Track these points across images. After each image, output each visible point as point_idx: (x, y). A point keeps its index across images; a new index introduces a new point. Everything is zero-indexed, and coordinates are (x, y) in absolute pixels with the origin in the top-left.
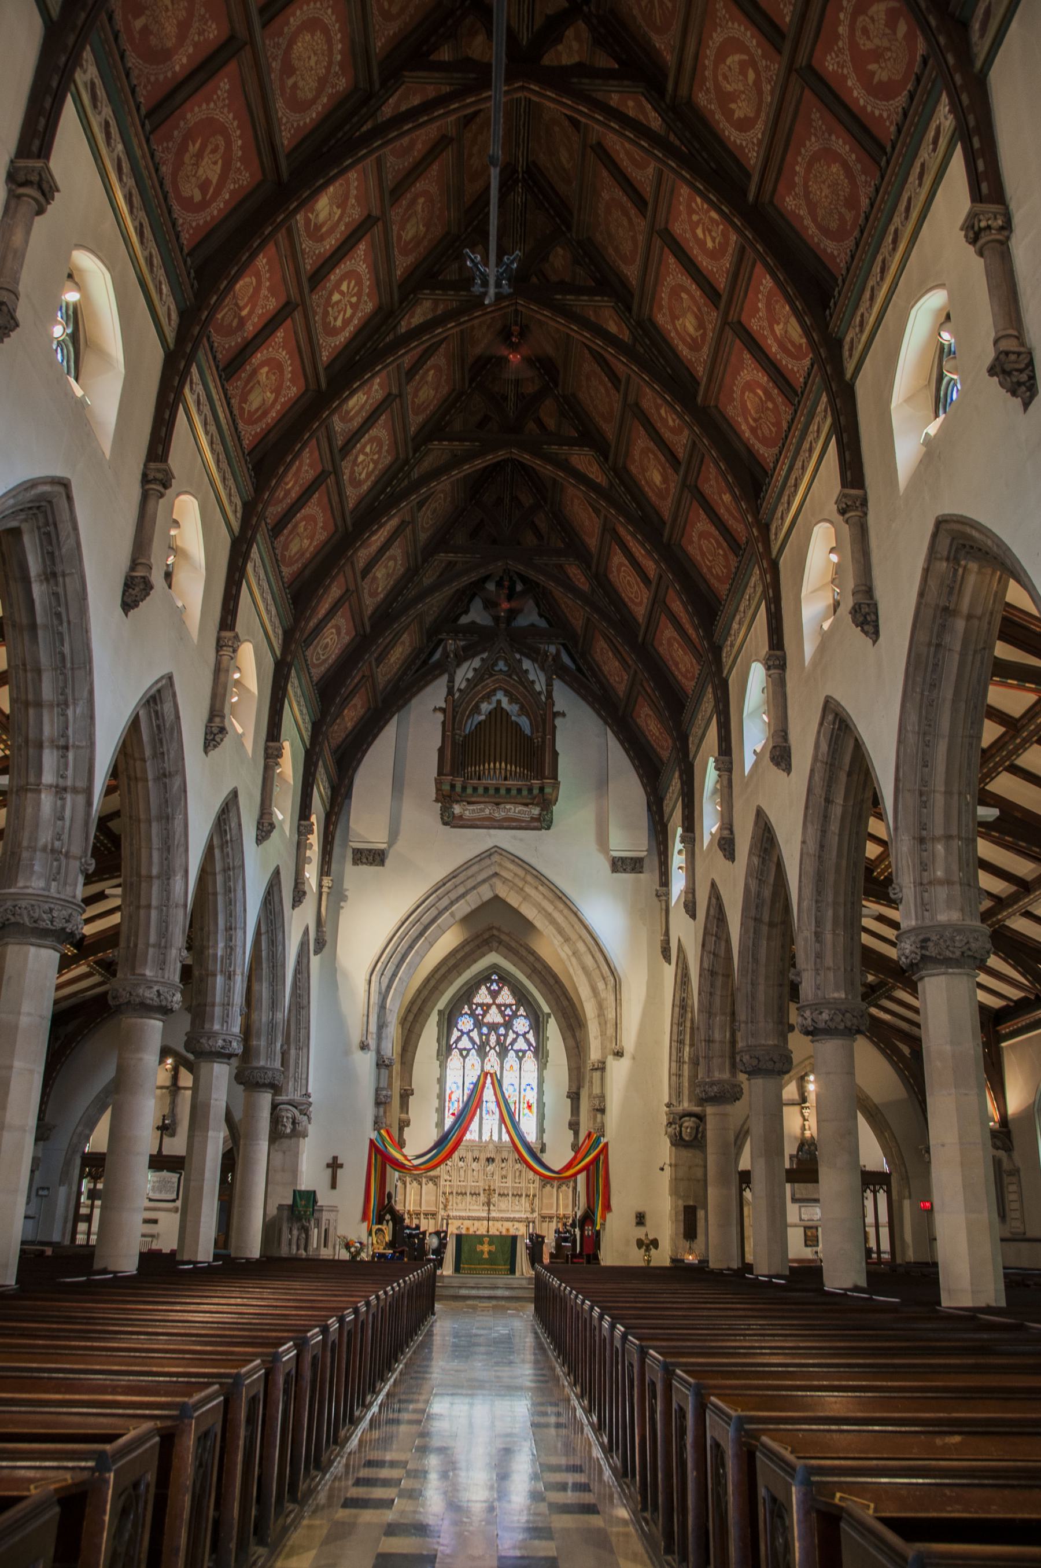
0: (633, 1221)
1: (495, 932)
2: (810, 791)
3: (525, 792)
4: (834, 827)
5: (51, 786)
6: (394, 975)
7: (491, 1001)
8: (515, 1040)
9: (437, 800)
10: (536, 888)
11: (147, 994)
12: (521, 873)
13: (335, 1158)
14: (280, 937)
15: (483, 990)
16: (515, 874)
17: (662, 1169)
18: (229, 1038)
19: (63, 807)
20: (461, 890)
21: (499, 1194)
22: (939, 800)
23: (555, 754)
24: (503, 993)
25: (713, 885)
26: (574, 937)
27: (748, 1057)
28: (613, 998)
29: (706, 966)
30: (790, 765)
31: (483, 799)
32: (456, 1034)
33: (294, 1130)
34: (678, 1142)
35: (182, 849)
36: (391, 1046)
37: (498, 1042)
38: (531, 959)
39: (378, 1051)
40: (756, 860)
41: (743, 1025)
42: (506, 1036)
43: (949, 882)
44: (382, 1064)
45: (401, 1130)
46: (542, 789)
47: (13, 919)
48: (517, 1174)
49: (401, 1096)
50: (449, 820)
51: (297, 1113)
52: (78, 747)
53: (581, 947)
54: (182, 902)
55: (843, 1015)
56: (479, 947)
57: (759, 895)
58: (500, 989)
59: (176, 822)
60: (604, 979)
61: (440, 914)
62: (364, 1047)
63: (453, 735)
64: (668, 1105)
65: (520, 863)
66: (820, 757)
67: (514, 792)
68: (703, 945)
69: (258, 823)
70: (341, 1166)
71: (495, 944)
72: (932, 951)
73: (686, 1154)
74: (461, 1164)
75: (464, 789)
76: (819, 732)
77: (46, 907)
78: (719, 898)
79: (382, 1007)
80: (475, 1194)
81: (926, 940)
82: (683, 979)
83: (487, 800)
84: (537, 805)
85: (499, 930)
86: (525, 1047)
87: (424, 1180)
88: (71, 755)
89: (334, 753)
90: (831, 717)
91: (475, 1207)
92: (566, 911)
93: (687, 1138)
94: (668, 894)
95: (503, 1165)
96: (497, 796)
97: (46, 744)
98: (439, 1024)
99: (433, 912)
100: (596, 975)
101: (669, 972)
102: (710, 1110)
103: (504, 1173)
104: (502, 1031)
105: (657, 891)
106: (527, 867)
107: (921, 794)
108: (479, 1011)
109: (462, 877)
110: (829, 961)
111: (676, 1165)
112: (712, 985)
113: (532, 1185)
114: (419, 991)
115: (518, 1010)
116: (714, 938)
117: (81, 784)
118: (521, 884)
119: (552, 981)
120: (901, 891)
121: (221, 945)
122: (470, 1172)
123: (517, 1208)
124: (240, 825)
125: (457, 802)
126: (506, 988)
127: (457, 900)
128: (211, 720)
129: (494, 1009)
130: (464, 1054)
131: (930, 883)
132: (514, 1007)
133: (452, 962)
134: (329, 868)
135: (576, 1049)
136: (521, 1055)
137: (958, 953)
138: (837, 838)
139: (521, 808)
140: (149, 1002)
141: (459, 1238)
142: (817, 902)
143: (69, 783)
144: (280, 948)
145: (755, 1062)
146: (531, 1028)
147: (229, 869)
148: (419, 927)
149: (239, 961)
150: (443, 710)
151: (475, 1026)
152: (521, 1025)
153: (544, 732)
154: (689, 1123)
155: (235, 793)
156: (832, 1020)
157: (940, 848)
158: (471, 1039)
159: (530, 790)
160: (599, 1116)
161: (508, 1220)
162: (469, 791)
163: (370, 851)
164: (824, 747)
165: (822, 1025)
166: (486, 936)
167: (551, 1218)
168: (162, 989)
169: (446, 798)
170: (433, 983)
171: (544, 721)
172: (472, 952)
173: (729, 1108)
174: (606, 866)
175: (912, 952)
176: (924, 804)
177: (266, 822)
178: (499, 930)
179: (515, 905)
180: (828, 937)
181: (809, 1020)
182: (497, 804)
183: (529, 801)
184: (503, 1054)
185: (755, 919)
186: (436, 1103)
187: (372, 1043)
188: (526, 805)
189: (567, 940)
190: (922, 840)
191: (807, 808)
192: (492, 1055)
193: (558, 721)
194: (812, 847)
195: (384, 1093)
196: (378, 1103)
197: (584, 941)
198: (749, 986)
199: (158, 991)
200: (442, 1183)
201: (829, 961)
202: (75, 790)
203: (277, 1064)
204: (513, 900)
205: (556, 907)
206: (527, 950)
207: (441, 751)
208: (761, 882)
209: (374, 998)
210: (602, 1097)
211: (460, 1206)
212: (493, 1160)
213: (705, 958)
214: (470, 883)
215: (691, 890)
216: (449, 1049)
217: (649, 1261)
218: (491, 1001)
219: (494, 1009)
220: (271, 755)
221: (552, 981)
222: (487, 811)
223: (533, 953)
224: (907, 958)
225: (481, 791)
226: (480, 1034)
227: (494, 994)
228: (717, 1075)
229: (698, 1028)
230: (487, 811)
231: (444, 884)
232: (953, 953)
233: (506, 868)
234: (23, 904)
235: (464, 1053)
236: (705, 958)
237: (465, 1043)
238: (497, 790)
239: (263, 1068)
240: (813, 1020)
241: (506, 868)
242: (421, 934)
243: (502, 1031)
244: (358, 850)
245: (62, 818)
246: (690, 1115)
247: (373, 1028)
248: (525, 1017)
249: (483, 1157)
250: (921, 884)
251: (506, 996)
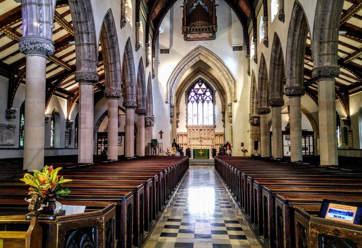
0: (241, 145)
1: (200, 69)
2: (290, 28)
3: (207, 30)
4: (297, 38)
5: (86, 44)
6: (173, 83)
7: (199, 88)
8: (206, 98)
9: (183, 34)
10: (211, 57)
11: (114, 93)
12: (207, 53)
13: (161, 131)
14: (143, 75)
15: (197, 84)
16: (206, 53)
17: (248, 132)
18: (134, 103)
19: (90, 49)
20: (191, 59)
22: (327, 31)
23: (216, 18)
24: (203, 85)
25: (262, 54)
26: (222, 70)
27: (271, 102)
28: (234, 86)
29: (260, 77)
30: (284, 20)
31: (196, 32)
32: (190, 97)
33: (150, 124)
34: (253, 124)
35: (118, 55)
36: (174, 102)
37: (202, 99)
38: (210, 76)
39: (170, 104)
40: (274, 47)
41: (270, 93)
42: (204, 97)
43: (328, 54)
44: (171, 107)
45: (177, 123)
46: (212, 28)
47: (82, 78)
48: (208, 133)
49: (177, 114)
50: (187, 39)
51: (151, 120)
52: (91, 33)
53: (225, 73)
54: (120, 70)
55: (298, 91)
56: (196, 74)
57: (275, 57)
58: (202, 84)
59: (116, 49)
60: (231, 81)
61: (185, 66)
62: (167, 102)
63: (186, 14)
64: (250, 115)
65: (207, 50)
66: (293, 18)
67: (204, 30)
68: (259, 71)
69: (136, 45)
70: (163, 133)
71: (200, 73)
72: (322, 74)
73: (255, 127)
74: (193, 131)
75: (190, 30)
76: (293, 11)
77: (89, 75)
78: (264, 58)
79: (171, 92)
81: (320, 71)
82: (254, 81)
83: (197, 32)
84: (211, 33)
85: (201, 68)
86: (209, 100)
88: (90, 35)
89: (153, 22)
90: (296, 6)
91: (197, 142)
92: (220, 63)
93: (255, 123)
94: (249, 56)
96: (200, 31)
97: (83, 33)
98: (185, 95)
99: (183, 65)
100: (229, 80)
101: (250, 78)
102: (261, 116)
104: (203, 96)
105: (246, 56)
106: (209, 51)
107: (321, 29)
108: (196, 90)
109: (190, 55)
110: (294, 76)
111: (252, 131)
112: (262, 82)
113: (212, 136)
114: (180, 87)
115: (207, 90)
116: (262, 69)
117: (93, 43)
118: (207, 56)
119: (216, 82)
120: (314, 57)
121: (129, 79)
124: (131, 47)
125: (188, 34)
126: (203, 84)
127: (189, 61)
128: (121, 19)
129: (200, 90)
130: (193, 102)
131: (322, 55)
132: (206, 89)
133: (188, 78)
134: (154, 55)
135: (224, 100)
136: (208, 102)
137: (329, 74)
138: (297, 41)
139: (206, 34)
140: (114, 95)
141: (194, 150)
142: (291, 59)
143: (90, 42)
144: (144, 78)
145: (273, 103)
146: (211, 94)
147: (129, 59)
148: (180, 70)
149: (134, 83)
150: (183, 7)
151: (195, 95)
152: (208, 94)
153: (212, 11)
154: (256, 119)
155: (129, 38)
156: (294, 92)
157: (326, 45)
158: (194, 98)
159: (209, 29)
160: (230, 118)
161: (206, 145)
162: (192, 30)
163: (165, 49)
164: (294, 15)
165: (292, 93)
166: (198, 71)
167: (218, 145)
168: (117, 92)
169: (185, 33)
170: (184, 84)
171: (212, 8)
172: (194, 75)
173: (267, 115)
174: (232, 49)
175: (316, 74)
176: (322, 32)
177: (138, 45)
178: (201, 68)
179: (206, 62)
180: (294, 69)
181: (288, 92)
182: (200, 33)
183: (209, 32)
184: (203, 102)
185: (274, 64)
186: (186, 116)
187: (169, 101)
188: (208, 33)
189: (221, 71)
190: (321, 43)
191: (289, 33)
192: (200, 103)
193: (217, 7)
194: (290, 44)
195: (173, 114)
196: (171, 117)
197: (225, 71)
198: (272, 83)
199: (116, 93)
200: (188, 136)
201: (294, 76)
202: (92, 44)
203: (145, 108)
204: (205, 60)
205: (217, 62)
206: (209, 74)
207: (183, 19)
208: (276, 53)
209: (169, 90)
210: (231, 113)
211: (193, 142)
212: (202, 130)
213: (260, 75)
214: (193, 57)
215: (256, 55)
216: (188, 101)
217: (245, 155)
218: (199, 88)
219: (200, 90)
220: (137, 26)
221: (216, 82)
222: (197, 36)
223: (211, 74)
224: (314, 76)
225: (195, 30)
226: (197, 97)
227: (200, 86)
228: (263, 107)
229: (258, 94)
230: (197, 36)
231: (186, 58)
232: (328, 74)
233: (203, 52)
234: (83, 74)
235: (193, 102)
236: (260, 75)
237: (193, 99)
238: (200, 29)
239: (142, 109)
240: (289, 92)
241: (203, 52)
242: (180, 72)
243: (203, 96)
244: (162, 49)
245: (90, 52)
246: (256, 117)
247: (169, 97)
248: (209, 92)
249: (199, 129)
250: (320, 55)
251: (204, 86)
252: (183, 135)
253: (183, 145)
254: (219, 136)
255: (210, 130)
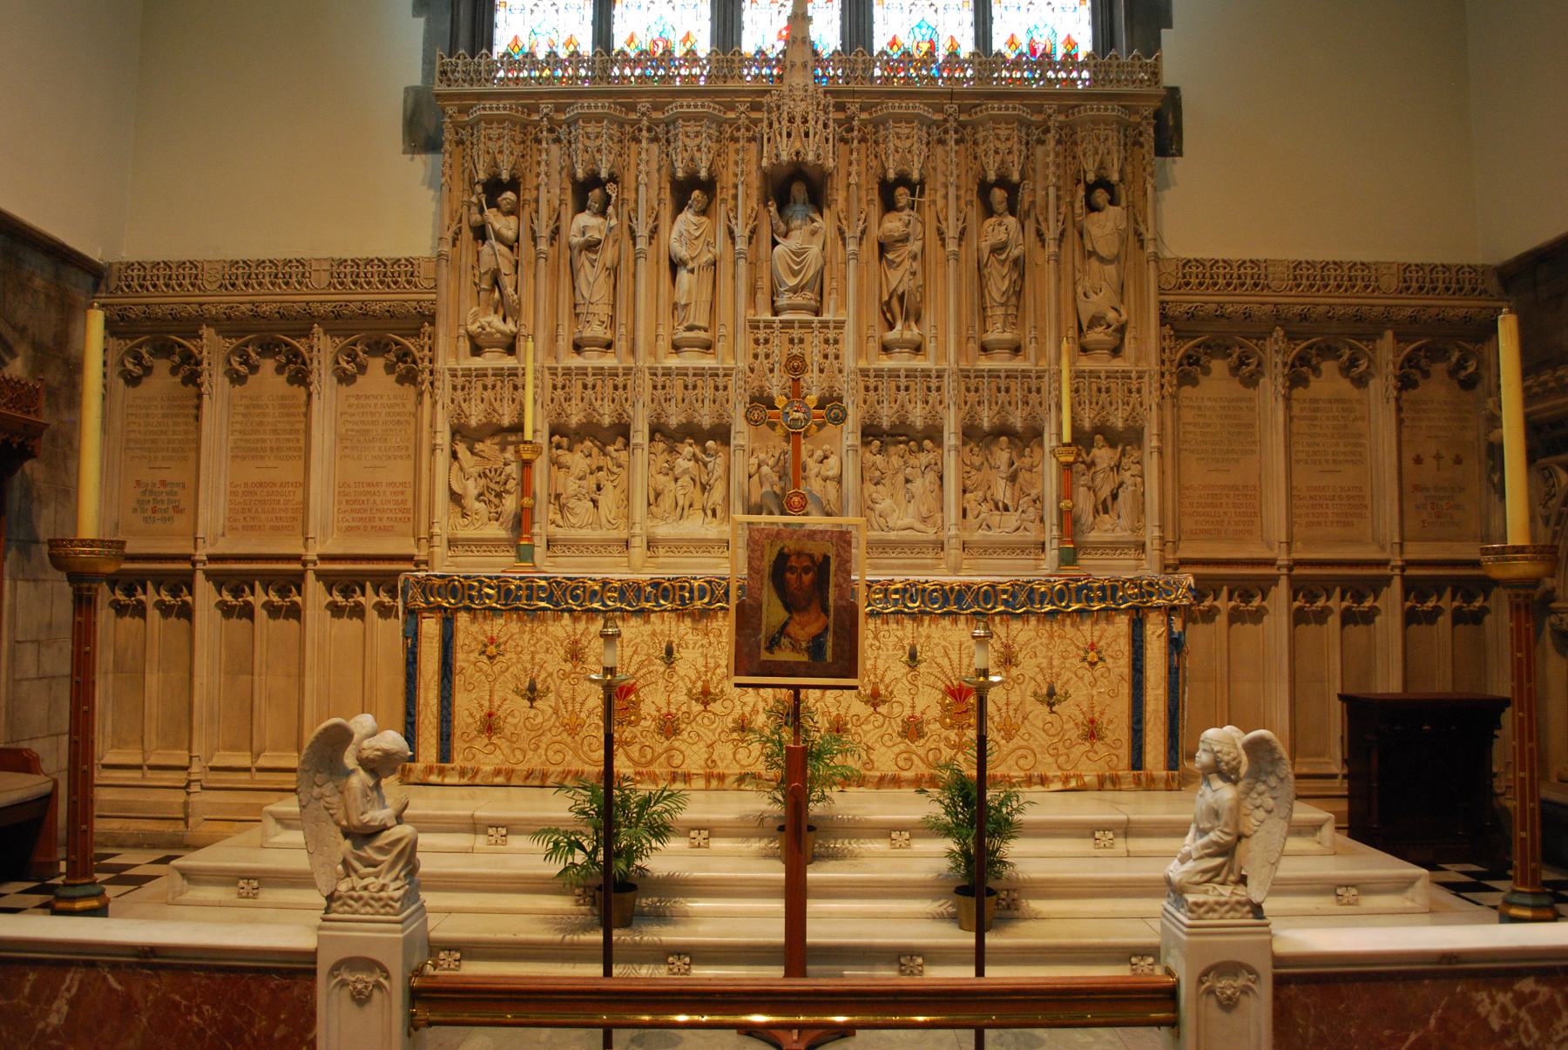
21: (870, 432)
48: (999, 284)
80: (692, 432)
87: (323, 350)
91: (696, 526)
95: (894, 224)
103: (898, 279)
122: (647, 277)
123: (1005, 527)
200: (450, 357)
211: (581, 523)
252: (303, 322)
253: (315, 596)
254: (1276, 354)
255: (1043, 189)
